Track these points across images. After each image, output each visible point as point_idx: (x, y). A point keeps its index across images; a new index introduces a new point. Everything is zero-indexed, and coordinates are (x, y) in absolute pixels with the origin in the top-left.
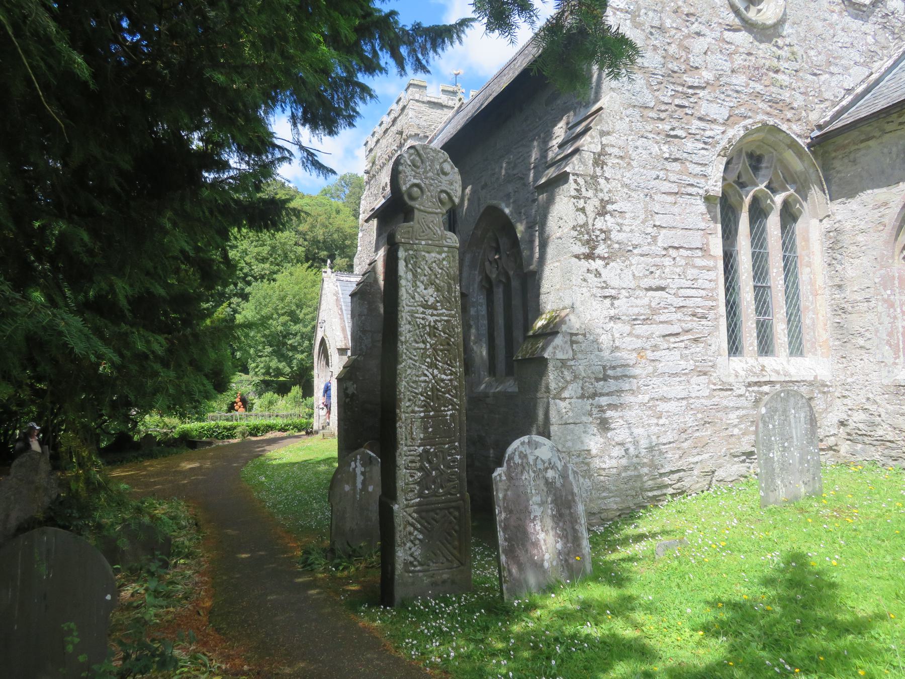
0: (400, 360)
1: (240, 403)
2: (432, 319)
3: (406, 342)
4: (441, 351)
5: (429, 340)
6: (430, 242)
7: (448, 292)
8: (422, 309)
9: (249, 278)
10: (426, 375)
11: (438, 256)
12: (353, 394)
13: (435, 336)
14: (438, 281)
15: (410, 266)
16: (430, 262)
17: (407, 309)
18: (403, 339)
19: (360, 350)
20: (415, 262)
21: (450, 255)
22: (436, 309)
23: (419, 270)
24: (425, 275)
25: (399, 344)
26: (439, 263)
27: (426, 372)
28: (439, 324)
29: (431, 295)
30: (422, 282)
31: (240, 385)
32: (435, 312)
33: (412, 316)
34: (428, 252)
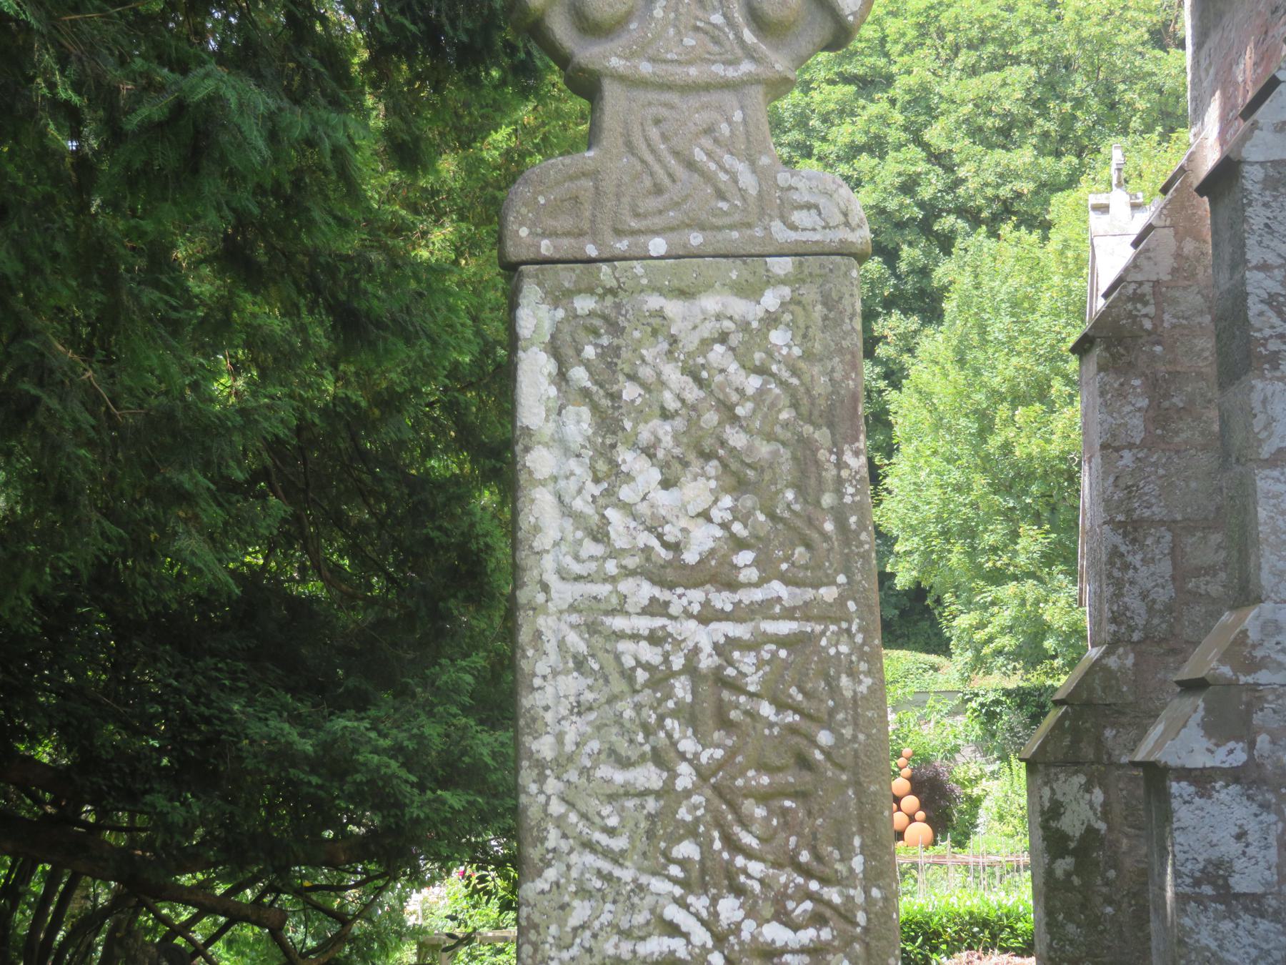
0: (534, 853)
1: (910, 802)
2: (703, 637)
3: (563, 762)
4: (764, 797)
5: (688, 745)
6: (696, 239)
7: (800, 489)
8: (646, 591)
9: (947, 222)
10: (673, 929)
11: (739, 307)
12: (1090, 831)
13: (726, 724)
14: (737, 439)
15: (579, 375)
16: (690, 342)
17: (564, 593)
18: (544, 747)
19: (1114, 620)
20: (610, 355)
21: (810, 293)
22: (733, 586)
23: (630, 392)
24: (666, 415)
25: (527, 777)
26: (746, 341)
27: (673, 913)
28: (746, 661)
29: (696, 512)
30: (649, 452)
31: (911, 716)
32: (723, 601)
33: (592, 628)
34: (684, 294)
